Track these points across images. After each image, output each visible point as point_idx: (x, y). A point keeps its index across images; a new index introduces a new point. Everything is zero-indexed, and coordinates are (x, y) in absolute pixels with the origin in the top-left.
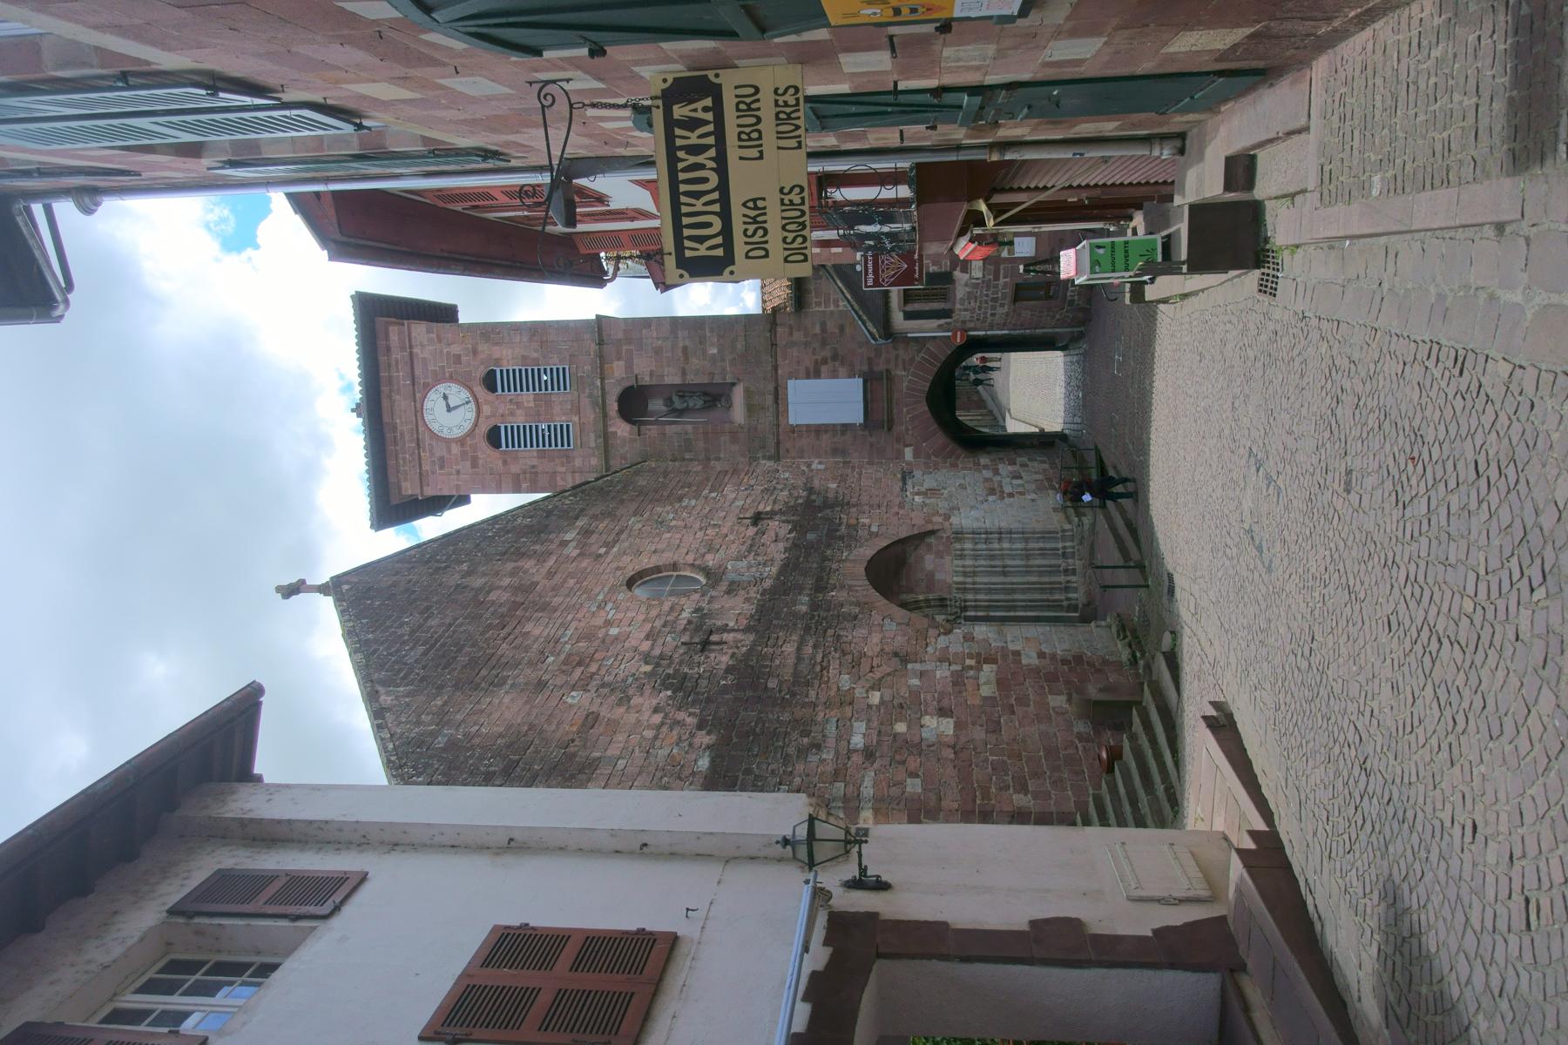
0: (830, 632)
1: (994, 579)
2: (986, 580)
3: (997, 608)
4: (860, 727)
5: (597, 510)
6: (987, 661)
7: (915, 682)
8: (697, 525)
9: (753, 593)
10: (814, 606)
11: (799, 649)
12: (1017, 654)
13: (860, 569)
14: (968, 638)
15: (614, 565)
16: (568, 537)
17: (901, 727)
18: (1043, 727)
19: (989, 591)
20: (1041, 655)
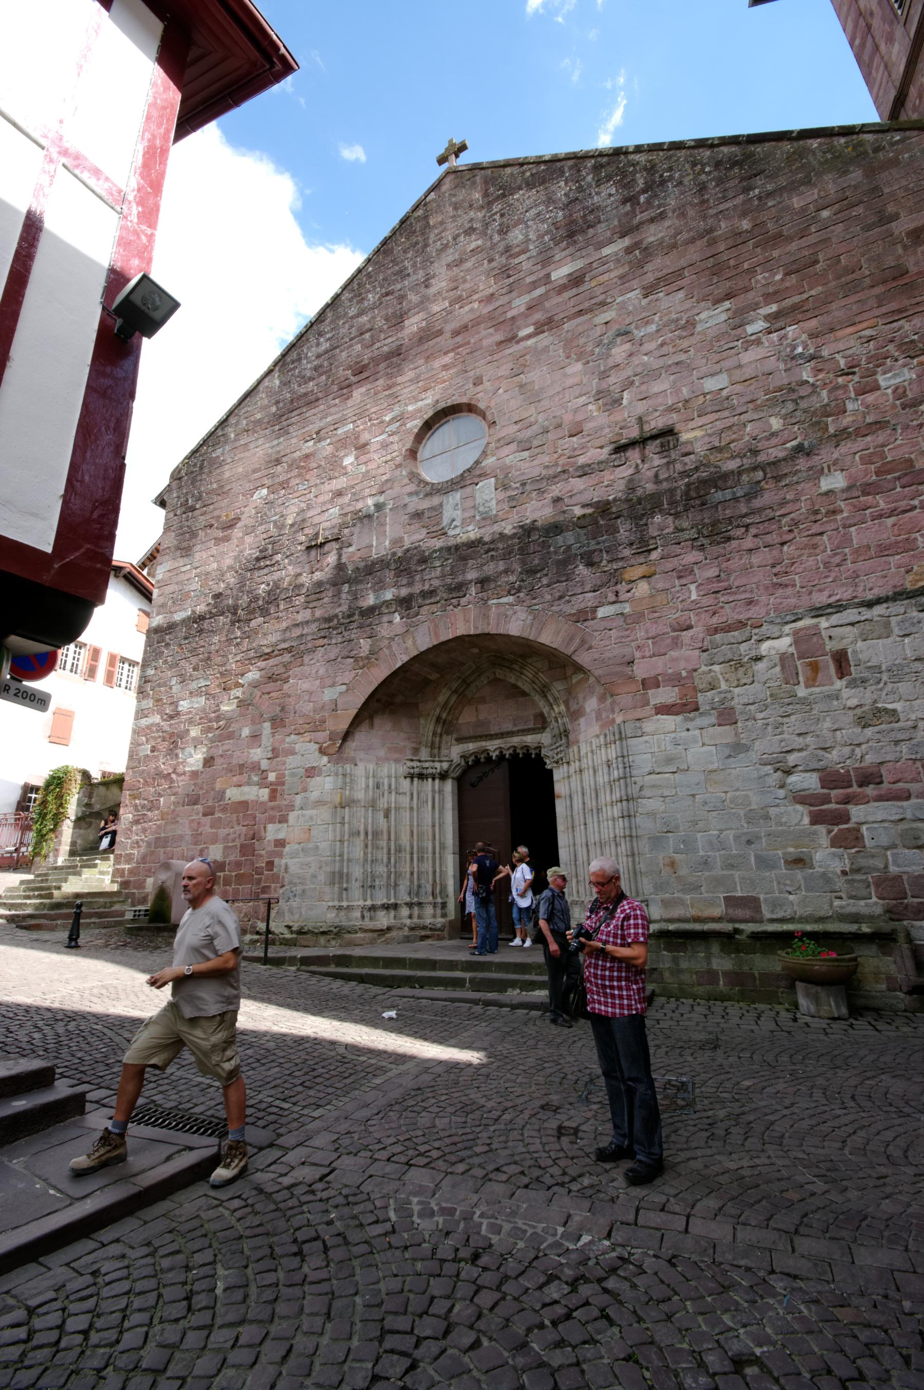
6: (273, 796)
12: (283, 820)
14: (311, 772)
17: (194, 732)
18: (188, 838)
20: (281, 843)
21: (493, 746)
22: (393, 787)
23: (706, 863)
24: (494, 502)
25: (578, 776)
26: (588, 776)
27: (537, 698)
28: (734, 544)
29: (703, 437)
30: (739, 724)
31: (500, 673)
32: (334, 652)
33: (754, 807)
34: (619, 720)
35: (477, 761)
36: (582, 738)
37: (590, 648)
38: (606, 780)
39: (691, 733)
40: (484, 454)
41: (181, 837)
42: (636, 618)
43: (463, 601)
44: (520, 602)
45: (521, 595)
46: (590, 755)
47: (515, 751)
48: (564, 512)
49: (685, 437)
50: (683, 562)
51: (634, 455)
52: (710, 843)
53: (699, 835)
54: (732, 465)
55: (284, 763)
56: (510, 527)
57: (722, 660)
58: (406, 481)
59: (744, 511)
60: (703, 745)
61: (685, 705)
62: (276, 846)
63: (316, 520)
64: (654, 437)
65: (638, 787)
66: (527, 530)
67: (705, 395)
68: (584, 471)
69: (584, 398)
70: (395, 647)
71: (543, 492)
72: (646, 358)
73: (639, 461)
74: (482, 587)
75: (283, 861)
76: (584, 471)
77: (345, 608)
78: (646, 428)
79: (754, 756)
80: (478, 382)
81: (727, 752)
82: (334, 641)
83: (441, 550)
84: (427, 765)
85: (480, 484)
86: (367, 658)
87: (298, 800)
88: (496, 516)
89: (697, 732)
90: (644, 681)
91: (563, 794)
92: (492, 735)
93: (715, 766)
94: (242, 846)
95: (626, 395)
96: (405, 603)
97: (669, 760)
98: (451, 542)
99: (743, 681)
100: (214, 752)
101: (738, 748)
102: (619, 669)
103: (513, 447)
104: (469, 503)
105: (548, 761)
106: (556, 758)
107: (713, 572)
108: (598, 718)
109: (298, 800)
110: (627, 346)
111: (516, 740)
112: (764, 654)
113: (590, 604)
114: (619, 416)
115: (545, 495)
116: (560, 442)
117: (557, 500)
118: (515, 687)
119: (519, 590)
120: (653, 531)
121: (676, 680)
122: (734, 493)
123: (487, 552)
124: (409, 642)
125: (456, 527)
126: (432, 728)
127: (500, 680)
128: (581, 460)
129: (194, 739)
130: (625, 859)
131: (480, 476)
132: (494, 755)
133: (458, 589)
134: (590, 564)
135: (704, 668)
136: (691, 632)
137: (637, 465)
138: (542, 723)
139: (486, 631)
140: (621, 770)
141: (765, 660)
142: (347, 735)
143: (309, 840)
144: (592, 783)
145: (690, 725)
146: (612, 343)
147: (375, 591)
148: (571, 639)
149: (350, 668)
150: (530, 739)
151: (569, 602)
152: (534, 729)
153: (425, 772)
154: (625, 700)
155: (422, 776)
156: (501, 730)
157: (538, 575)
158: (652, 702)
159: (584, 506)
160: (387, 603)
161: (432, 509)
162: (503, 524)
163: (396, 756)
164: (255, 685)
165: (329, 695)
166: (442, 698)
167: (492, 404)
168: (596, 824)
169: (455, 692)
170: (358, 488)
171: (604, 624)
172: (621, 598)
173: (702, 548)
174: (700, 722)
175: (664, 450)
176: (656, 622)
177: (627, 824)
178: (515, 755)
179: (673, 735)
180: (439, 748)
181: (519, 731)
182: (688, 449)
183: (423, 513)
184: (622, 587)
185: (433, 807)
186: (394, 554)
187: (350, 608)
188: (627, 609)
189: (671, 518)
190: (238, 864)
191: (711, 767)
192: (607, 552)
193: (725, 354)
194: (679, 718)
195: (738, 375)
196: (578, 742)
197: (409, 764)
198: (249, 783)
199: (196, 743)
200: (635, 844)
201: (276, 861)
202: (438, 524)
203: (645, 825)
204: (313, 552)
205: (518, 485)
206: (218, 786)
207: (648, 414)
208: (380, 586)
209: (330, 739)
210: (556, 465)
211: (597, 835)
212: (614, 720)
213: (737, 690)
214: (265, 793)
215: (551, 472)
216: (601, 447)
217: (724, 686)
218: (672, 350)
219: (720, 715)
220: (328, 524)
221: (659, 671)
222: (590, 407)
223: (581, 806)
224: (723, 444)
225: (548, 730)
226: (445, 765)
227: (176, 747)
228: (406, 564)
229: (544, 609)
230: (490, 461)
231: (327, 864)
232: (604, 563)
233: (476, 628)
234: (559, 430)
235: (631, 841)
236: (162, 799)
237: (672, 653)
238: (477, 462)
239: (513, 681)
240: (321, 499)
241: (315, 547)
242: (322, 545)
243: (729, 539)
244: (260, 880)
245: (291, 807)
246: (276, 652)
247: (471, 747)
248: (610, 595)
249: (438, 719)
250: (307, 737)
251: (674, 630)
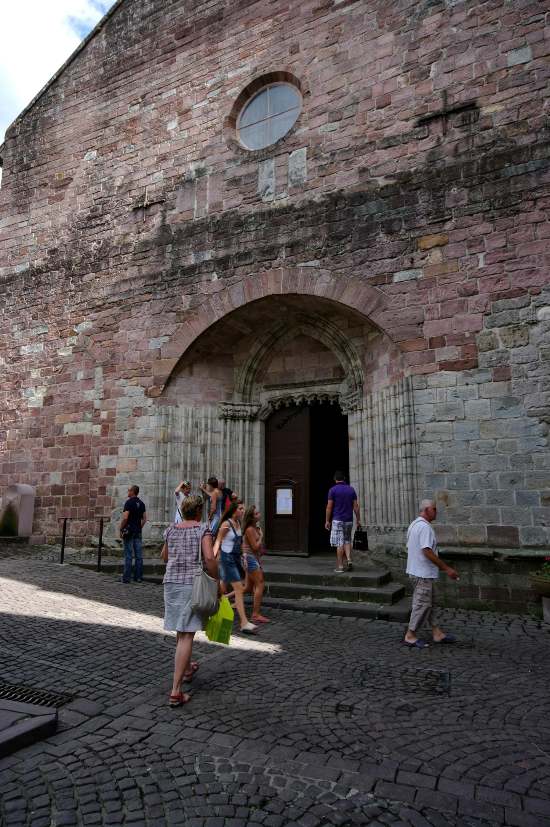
6: (105, 431)
12: (114, 452)
14: (138, 412)
17: (35, 374)
18: (32, 465)
20: (112, 472)
21: (296, 393)
22: (209, 426)
23: (474, 499)
24: (305, 171)
25: (369, 422)
26: (378, 423)
27: (337, 353)
28: (522, 216)
29: (502, 111)
30: (513, 381)
31: (305, 329)
32: (158, 306)
33: (519, 452)
34: (407, 374)
35: (282, 406)
36: (374, 389)
37: (386, 309)
38: (394, 425)
39: (469, 387)
40: (298, 123)
41: (26, 464)
42: (428, 284)
43: (275, 263)
44: (325, 265)
45: (327, 259)
46: (380, 403)
47: (316, 398)
48: (369, 182)
49: (486, 111)
50: (474, 233)
51: (436, 128)
52: (479, 482)
53: (470, 475)
54: (526, 140)
55: (115, 404)
56: (319, 195)
57: (502, 323)
58: (225, 148)
59: (534, 185)
60: (480, 397)
61: (466, 362)
62: (107, 474)
63: (142, 183)
64: (456, 111)
65: (419, 433)
66: (335, 199)
67: (508, 69)
68: (389, 143)
69: (393, 69)
70: (212, 303)
71: (351, 163)
72: (455, 29)
73: (441, 135)
74: (292, 251)
75: (114, 487)
76: (389, 143)
77: (168, 267)
78: (450, 101)
79: (522, 409)
80: (294, 50)
81: (500, 405)
82: (158, 297)
83: (255, 215)
84: (239, 408)
85: (293, 153)
86: (188, 312)
87: (127, 435)
88: (307, 184)
89: (475, 387)
90: (431, 340)
91: (356, 436)
92: (296, 384)
93: (488, 416)
94: (79, 473)
95: (433, 67)
96: (222, 264)
97: (449, 410)
98: (266, 208)
99: (519, 343)
100: (52, 391)
101: (510, 401)
102: (410, 329)
103: (325, 117)
104: (282, 171)
105: (344, 408)
106: (351, 405)
107: (500, 242)
108: (389, 371)
109: (127, 435)
110: (438, 17)
111: (316, 389)
112: (540, 318)
113: (387, 269)
114: (425, 88)
115: (353, 166)
116: (369, 113)
117: (363, 171)
118: (318, 342)
119: (325, 255)
120: (449, 203)
121: (459, 340)
122: (526, 168)
123: (297, 219)
124: (226, 300)
125: (270, 194)
126: (244, 376)
127: (305, 336)
128: (388, 132)
129: (35, 380)
130: (406, 493)
131: (293, 145)
132: (297, 401)
133: (271, 252)
134: (390, 232)
135: (485, 330)
136: (476, 298)
137: (439, 139)
138: (340, 375)
139: (294, 291)
140: (407, 418)
141: (540, 324)
142: (169, 381)
143: (136, 470)
144: (381, 428)
145: (469, 380)
146: (423, 14)
147: (195, 252)
148: (370, 300)
149: (172, 321)
150: (329, 389)
151: (369, 266)
152: (333, 380)
153: (237, 414)
154: (413, 356)
155: (234, 418)
156: (304, 380)
157: (343, 242)
158: (438, 359)
159: (387, 177)
160: (206, 263)
161: (248, 176)
162: (313, 192)
163: (213, 400)
164: (88, 334)
165: (154, 344)
166: (253, 351)
167: (307, 73)
168: (382, 463)
169: (265, 345)
170: (181, 153)
171: (399, 288)
172: (416, 264)
173: (492, 220)
174: (478, 377)
175: (465, 124)
176: (446, 288)
177: (409, 464)
178: (315, 402)
179: (454, 389)
180: (250, 394)
181: (320, 381)
182: (488, 123)
183: (240, 180)
184: (417, 255)
185: (244, 445)
186: (213, 218)
187: (173, 266)
188: (421, 274)
189: (466, 191)
190: (75, 489)
191: (485, 417)
192: (406, 221)
193: (530, 27)
194: (460, 374)
195: (541, 49)
196: (371, 392)
197: (224, 407)
198: (84, 420)
199: (37, 384)
200: (415, 480)
201: (108, 486)
202: (254, 190)
203: (425, 465)
204: (140, 214)
205: (328, 155)
206: (57, 421)
207: (452, 87)
208: (200, 248)
210: (364, 136)
211: (383, 472)
212: (403, 374)
213: (513, 351)
214: (97, 429)
215: (359, 143)
216: (407, 120)
217: (501, 347)
218: (480, 22)
219: (496, 372)
220: (153, 188)
221: (446, 331)
222: (399, 79)
223: (370, 447)
224: (520, 119)
225: (345, 381)
226: (255, 409)
227: (19, 387)
228: (224, 227)
229: (346, 273)
230: (303, 131)
231: (151, 490)
232: (403, 231)
233: (285, 288)
234: (368, 101)
235: (412, 478)
236: (8, 432)
237: (458, 316)
238: (291, 132)
239: (316, 337)
240: (147, 163)
241: (142, 208)
242: (148, 207)
243: (518, 212)
244: (94, 502)
245: (121, 442)
246: (107, 305)
247: (278, 393)
248: (406, 261)
249: (250, 368)
250: (135, 381)
251: (461, 295)
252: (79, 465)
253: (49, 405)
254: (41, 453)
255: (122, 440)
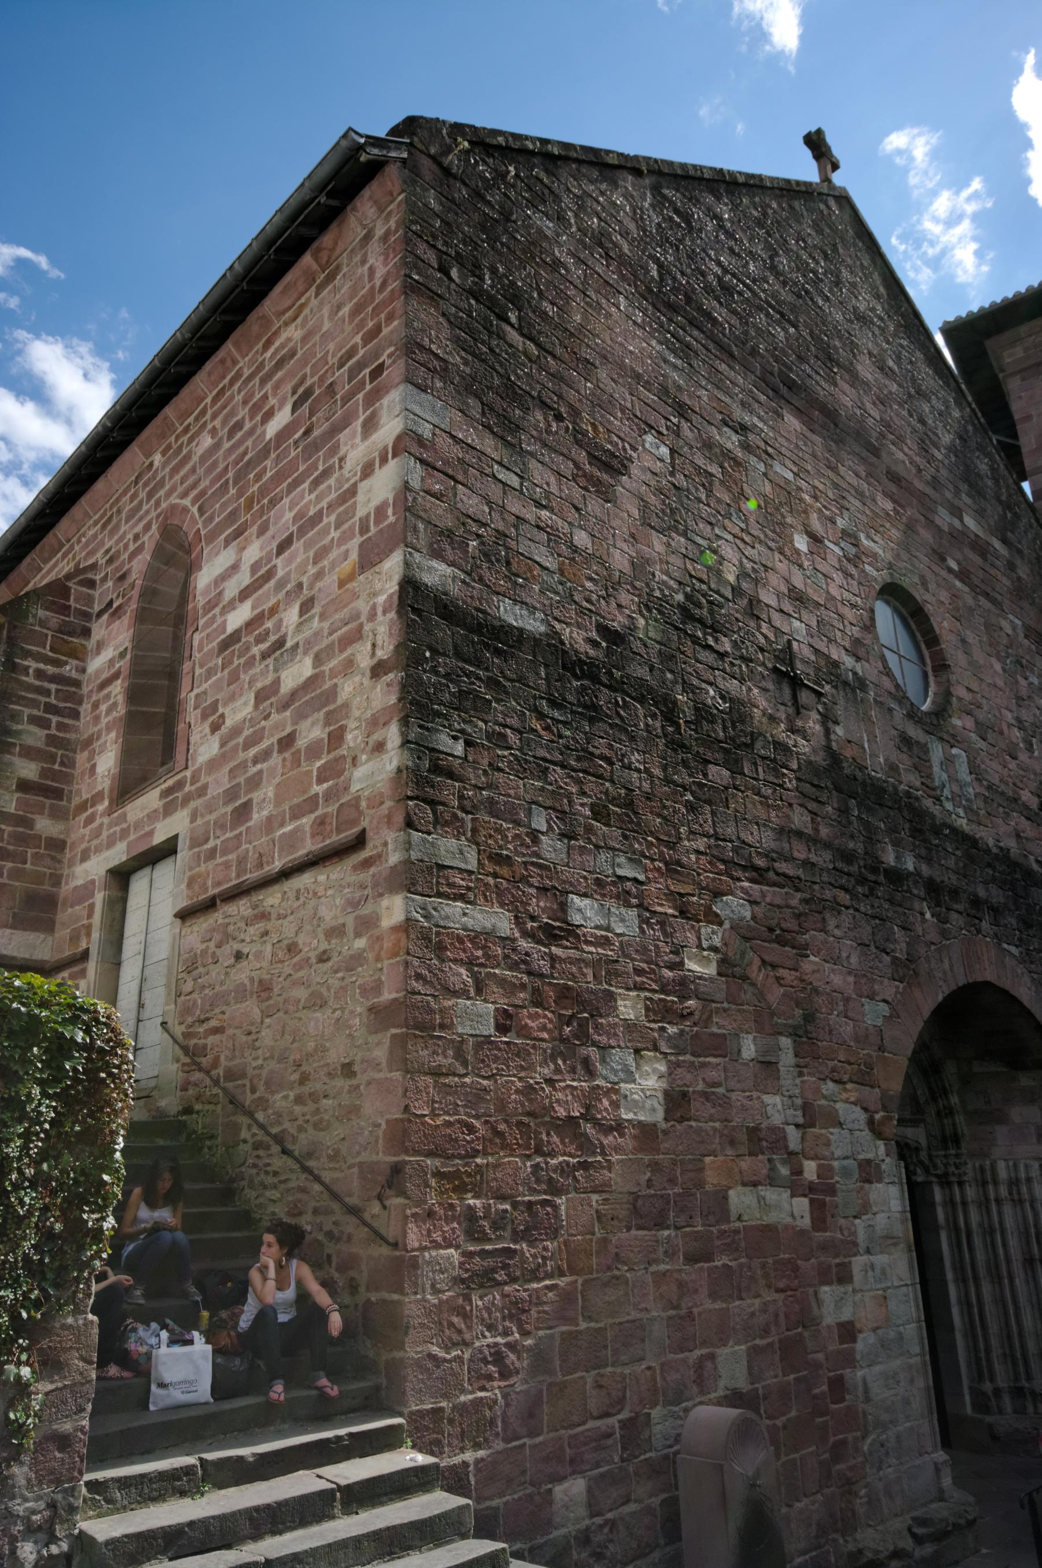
0: (844, 898)
1: (1013, 1242)
2: (1009, 1223)
3: (956, 1245)
4: (625, 923)
5: (1023, 571)
7: (749, 1048)
8: (1026, 715)
9: (910, 779)
10: (896, 877)
11: (799, 834)
13: (989, 975)
15: (929, 576)
16: (970, 521)
17: (629, 1007)
19: (989, 1232)
55: (828, 1144)
129: (630, 1026)
164: (743, 933)
198: (772, 1181)
209: (885, 1108)
236: (561, 1201)
245: (851, 1246)
246: (771, 875)
250: (853, 1092)
252: (782, 1318)
253: (682, 1119)
254: (681, 1285)
255: (855, 1244)
